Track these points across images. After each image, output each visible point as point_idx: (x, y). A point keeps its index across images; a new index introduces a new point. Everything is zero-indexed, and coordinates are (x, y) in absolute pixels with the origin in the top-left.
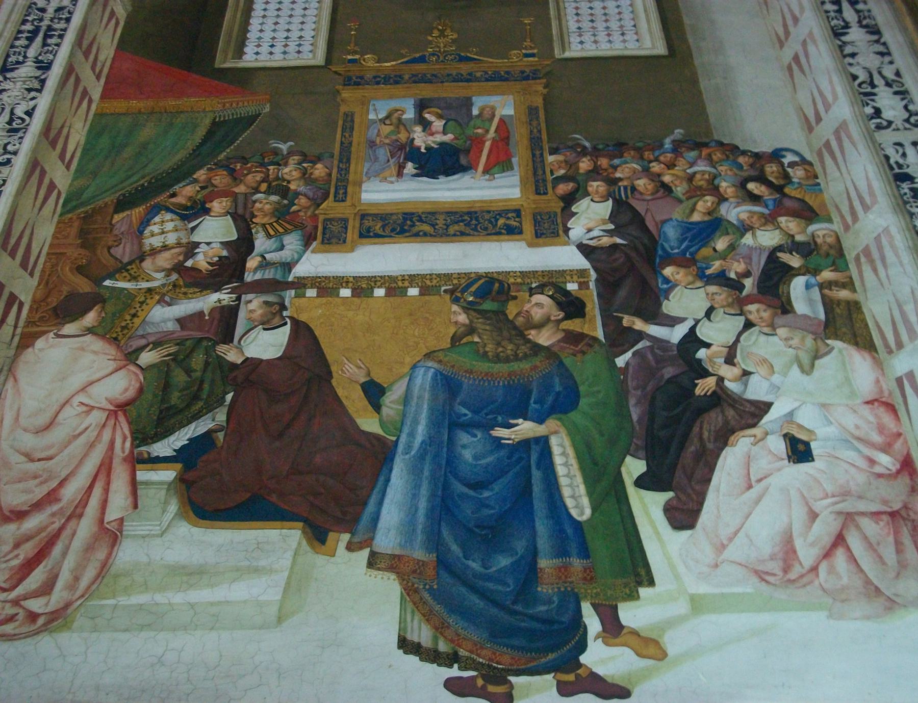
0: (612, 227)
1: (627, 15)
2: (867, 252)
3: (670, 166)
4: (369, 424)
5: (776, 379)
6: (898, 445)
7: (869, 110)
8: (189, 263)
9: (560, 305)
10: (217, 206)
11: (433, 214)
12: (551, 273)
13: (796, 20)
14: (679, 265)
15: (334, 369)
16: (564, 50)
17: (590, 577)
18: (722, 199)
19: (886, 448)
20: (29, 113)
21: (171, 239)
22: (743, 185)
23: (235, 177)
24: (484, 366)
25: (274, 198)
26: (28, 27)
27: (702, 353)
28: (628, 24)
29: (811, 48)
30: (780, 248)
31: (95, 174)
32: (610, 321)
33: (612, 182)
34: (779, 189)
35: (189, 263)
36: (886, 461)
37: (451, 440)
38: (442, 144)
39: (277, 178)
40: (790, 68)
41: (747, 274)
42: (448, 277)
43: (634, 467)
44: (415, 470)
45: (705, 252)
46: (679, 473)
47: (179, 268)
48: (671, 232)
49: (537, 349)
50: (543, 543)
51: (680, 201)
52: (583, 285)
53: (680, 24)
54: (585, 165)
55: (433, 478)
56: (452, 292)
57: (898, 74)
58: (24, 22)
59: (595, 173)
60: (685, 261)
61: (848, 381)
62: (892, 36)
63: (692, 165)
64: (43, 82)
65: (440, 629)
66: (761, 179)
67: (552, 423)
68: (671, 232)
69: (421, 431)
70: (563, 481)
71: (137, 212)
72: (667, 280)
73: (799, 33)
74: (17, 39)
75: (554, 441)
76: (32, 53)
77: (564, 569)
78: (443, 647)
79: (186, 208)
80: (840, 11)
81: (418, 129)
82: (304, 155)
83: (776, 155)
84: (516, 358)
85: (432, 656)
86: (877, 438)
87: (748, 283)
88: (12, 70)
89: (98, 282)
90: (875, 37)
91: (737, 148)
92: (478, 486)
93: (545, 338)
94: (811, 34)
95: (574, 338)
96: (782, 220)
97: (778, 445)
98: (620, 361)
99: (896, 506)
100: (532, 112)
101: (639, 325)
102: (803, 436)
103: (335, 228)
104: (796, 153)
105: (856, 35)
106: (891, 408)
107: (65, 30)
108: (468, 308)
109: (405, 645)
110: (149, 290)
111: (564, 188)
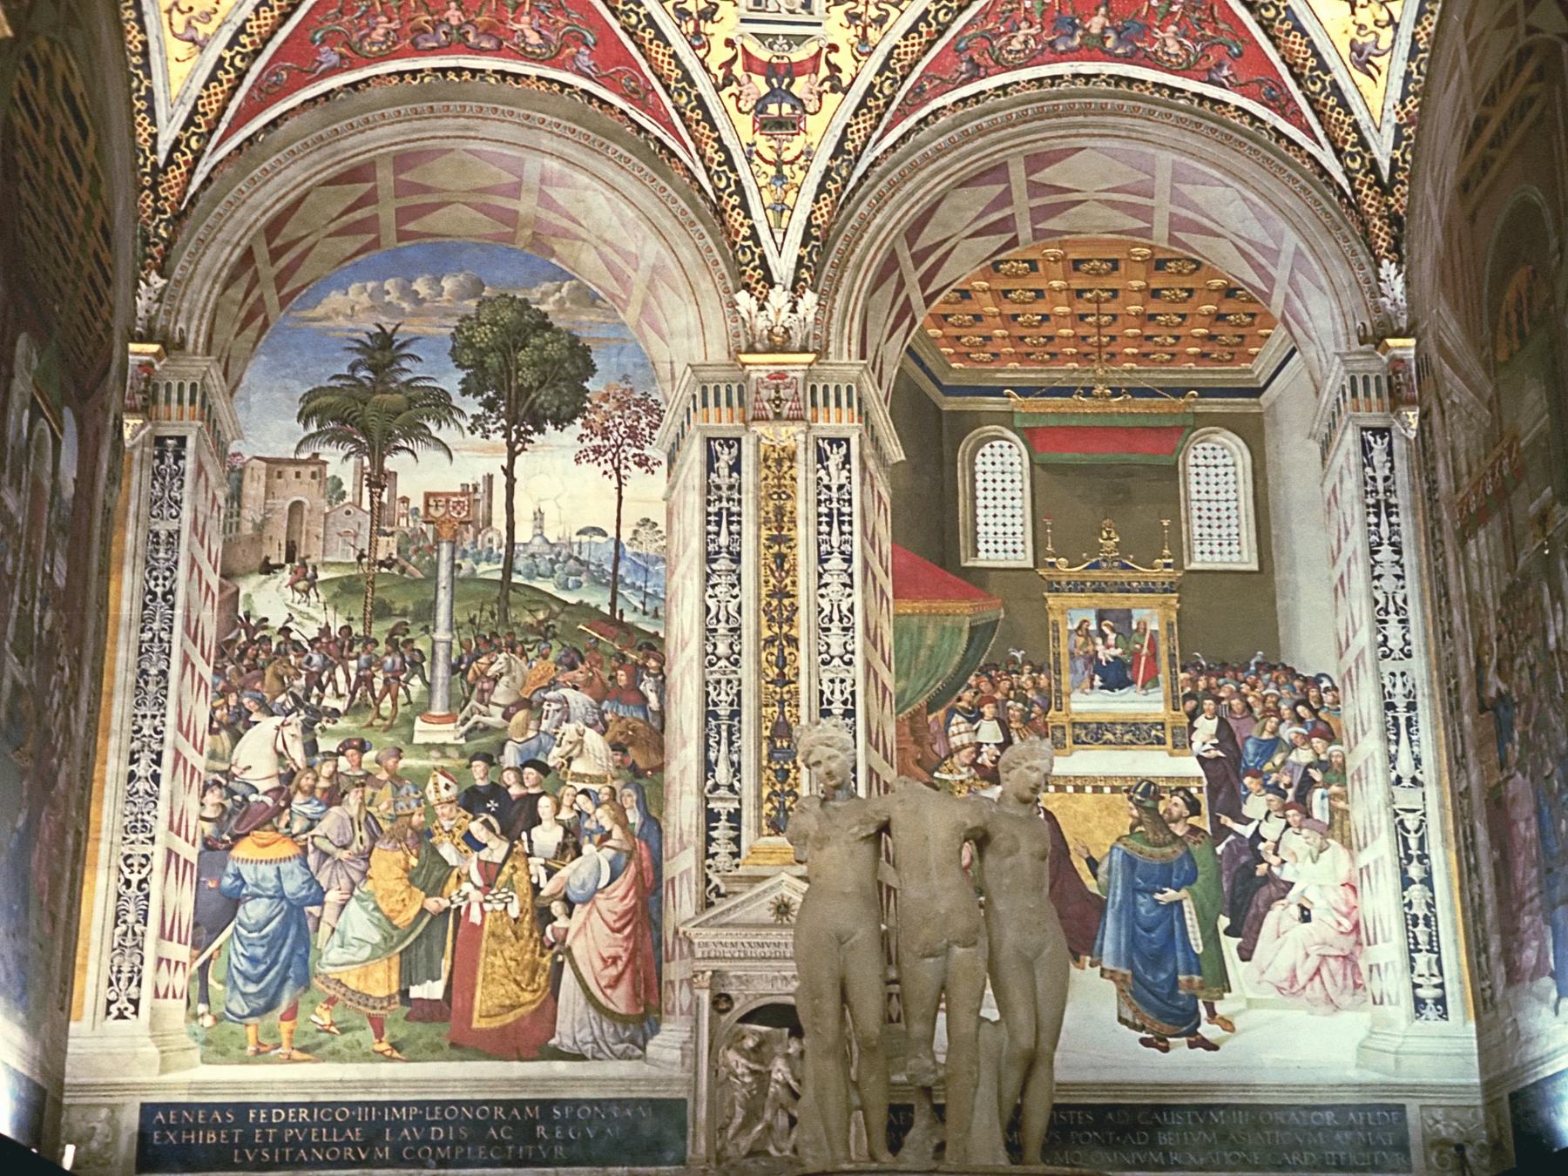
0: (1216, 741)
1: (1233, 521)
2: (1359, 770)
3: (1253, 687)
4: (1091, 884)
5: (1298, 866)
6: (1354, 914)
7: (1380, 638)
8: (979, 761)
9: (1188, 805)
10: (988, 710)
11: (1113, 724)
12: (1181, 778)
13: (1347, 533)
14: (1255, 777)
15: (1071, 847)
16: (1190, 560)
17: (1202, 988)
18: (1282, 721)
19: (1347, 916)
20: (851, 610)
21: (966, 739)
22: (1294, 709)
23: (995, 686)
24: (1148, 849)
25: (1020, 705)
26: (823, 510)
27: (1261, 846)
28: (1234, 530)
29: (1353, 567)
30: (1309, 765)
31: (908, 675)
32: (1215, 820)
33: (1218, 700)
34: (1315, 712)
35: (979, 761)
36: (1347, 925)
37: (1135, 902)
38: (1115, 658)
39: (1020, 687)
40: (1336, 589)
41: (1289, 786)
42: (1124, 778)
43: (1224, 922)
44: (1118, 920)
45: (1268, 766)
46: (1245, 929)
47: (974, 764)
48: (1250, 747)
49: (1175, 837)
50: (1181, 965)
51: (1257, 721)
52: (1200, 790)
53: (1269, 535)
54: (1202, 684)
55: (1127, 926)
56: (1127, 791)
57: (1405, 601)
58: (819, 502)
59: (1209, 692)
60: (1257, 774)
61: (1334, 870)
62: (1409, 558)
63: (1266, 687)
64: (851, 575)
65: (1136, 1012)
66: (1306, 703)
67: (1183, 893)
68: (1250, 747)
69: (1119, 892)
70: (1190, 929)
71: (941, 713)
72: (1246, 788)
73: (1347, 548)
74: (820, 523)
75: (1185, 903)
76: (835, 543)
77: (1190, 981)
78: (1138, 1022)
79: (970, 712)
80: (1378, 525)
81: (1099, 641)
82: (1031, 663)
83: (1317, 680)
84: (1165, 845)
85: (1134, 1027)
86: (1344, 909)
87: (1290, 792)
88: (827, 561)
89: (931, 773)
90: (1397, 557)
91: (1293, 670)
92: (1148, 930)
93: (1179, 830)
94: (1355, 552)
95: (1194, 830)
96: (1315, 740)
97: (1295, 911)
98: (1219, 850)
99: (1347, 952)
100: (1170, 625)
101: (1229, 823)
102: (1307, 905)
103: (1058, 734)
104: (1330, 680)
105: (1386, 553)
106: (1354, 889)
107: (850, 515)
108: (1138, 804)
109: (1121, 1020)
110: (962, 782)
111: (1191, 704)
